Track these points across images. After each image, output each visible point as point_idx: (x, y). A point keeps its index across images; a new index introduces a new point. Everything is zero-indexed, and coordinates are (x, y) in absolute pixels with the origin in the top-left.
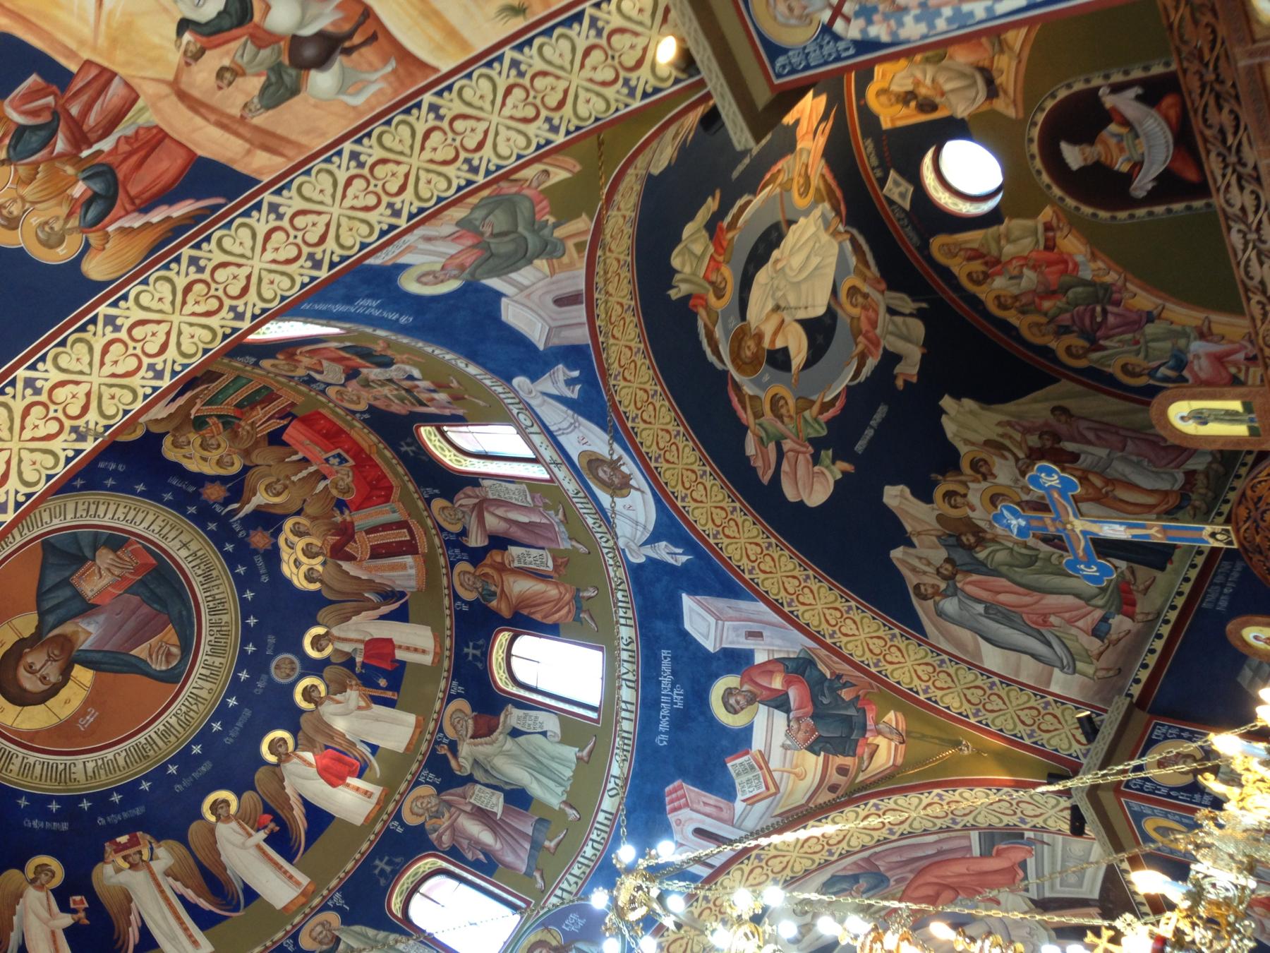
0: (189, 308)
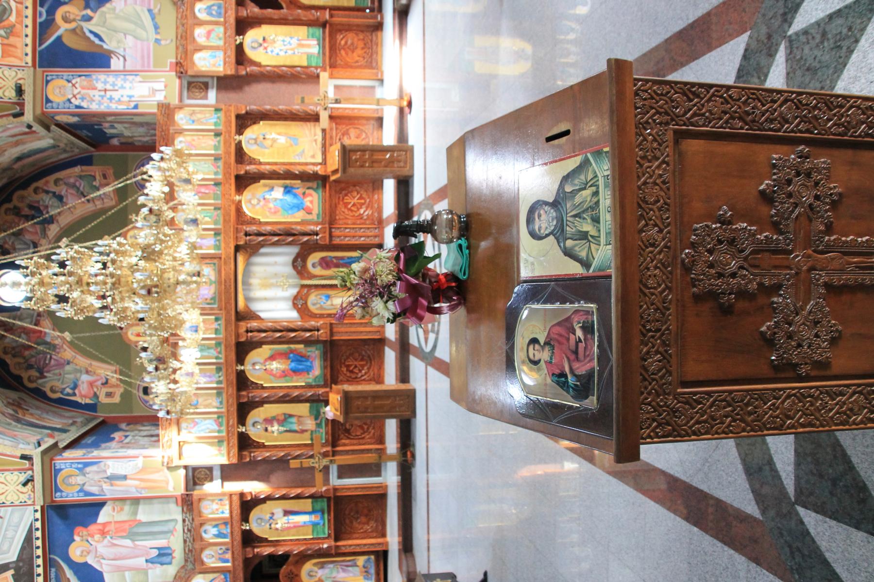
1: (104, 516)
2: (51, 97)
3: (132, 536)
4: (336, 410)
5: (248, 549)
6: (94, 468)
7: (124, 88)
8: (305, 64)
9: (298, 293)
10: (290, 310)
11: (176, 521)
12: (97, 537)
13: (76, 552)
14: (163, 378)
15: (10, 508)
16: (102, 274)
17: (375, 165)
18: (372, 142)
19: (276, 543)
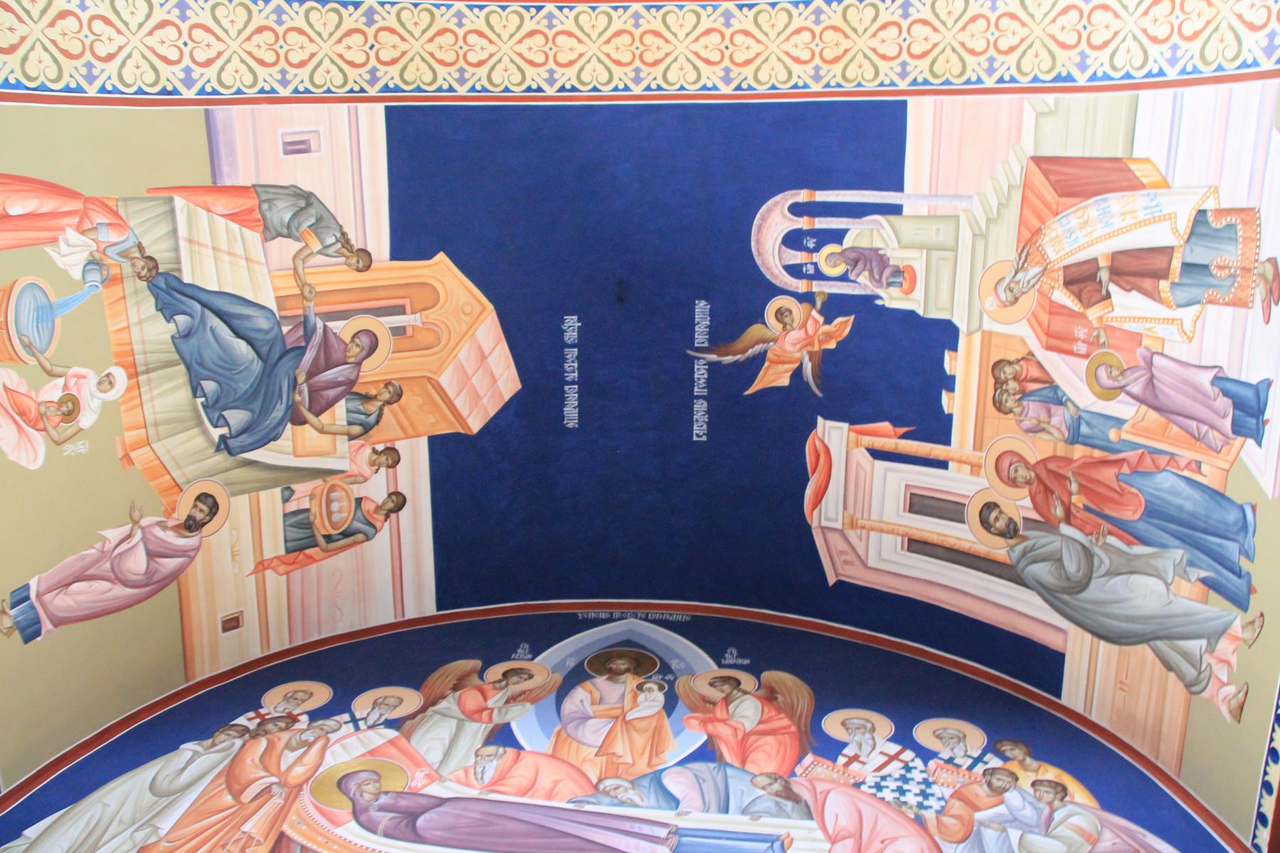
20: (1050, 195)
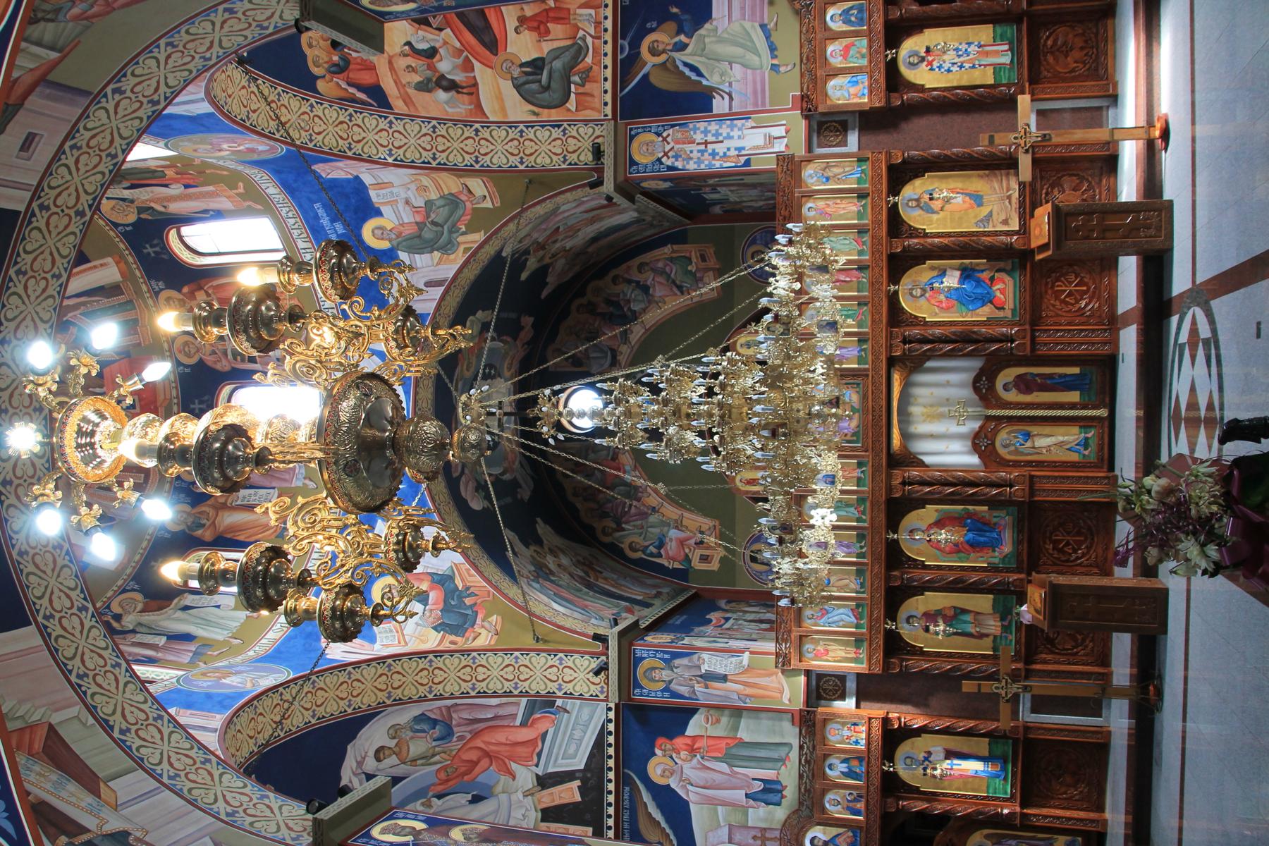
0: (337, 129)
1: (695, 727)
2: (636, 158)
3: (729, 758)
4: (1036, 611)
5: (889, 800)
6: (684, 661)
7: (732, 138)
8: (991, 81)
9: (981, 428)
10: (968, 453)
11: (789, 745)
12: (683, 754)
13: (656, 770)
14: (789, 554)
15: (578, 702)
16: (708, 403)
17: (1108, 234)
18: (1101, 197)
19: (932, 797)
20: (38, 745)
